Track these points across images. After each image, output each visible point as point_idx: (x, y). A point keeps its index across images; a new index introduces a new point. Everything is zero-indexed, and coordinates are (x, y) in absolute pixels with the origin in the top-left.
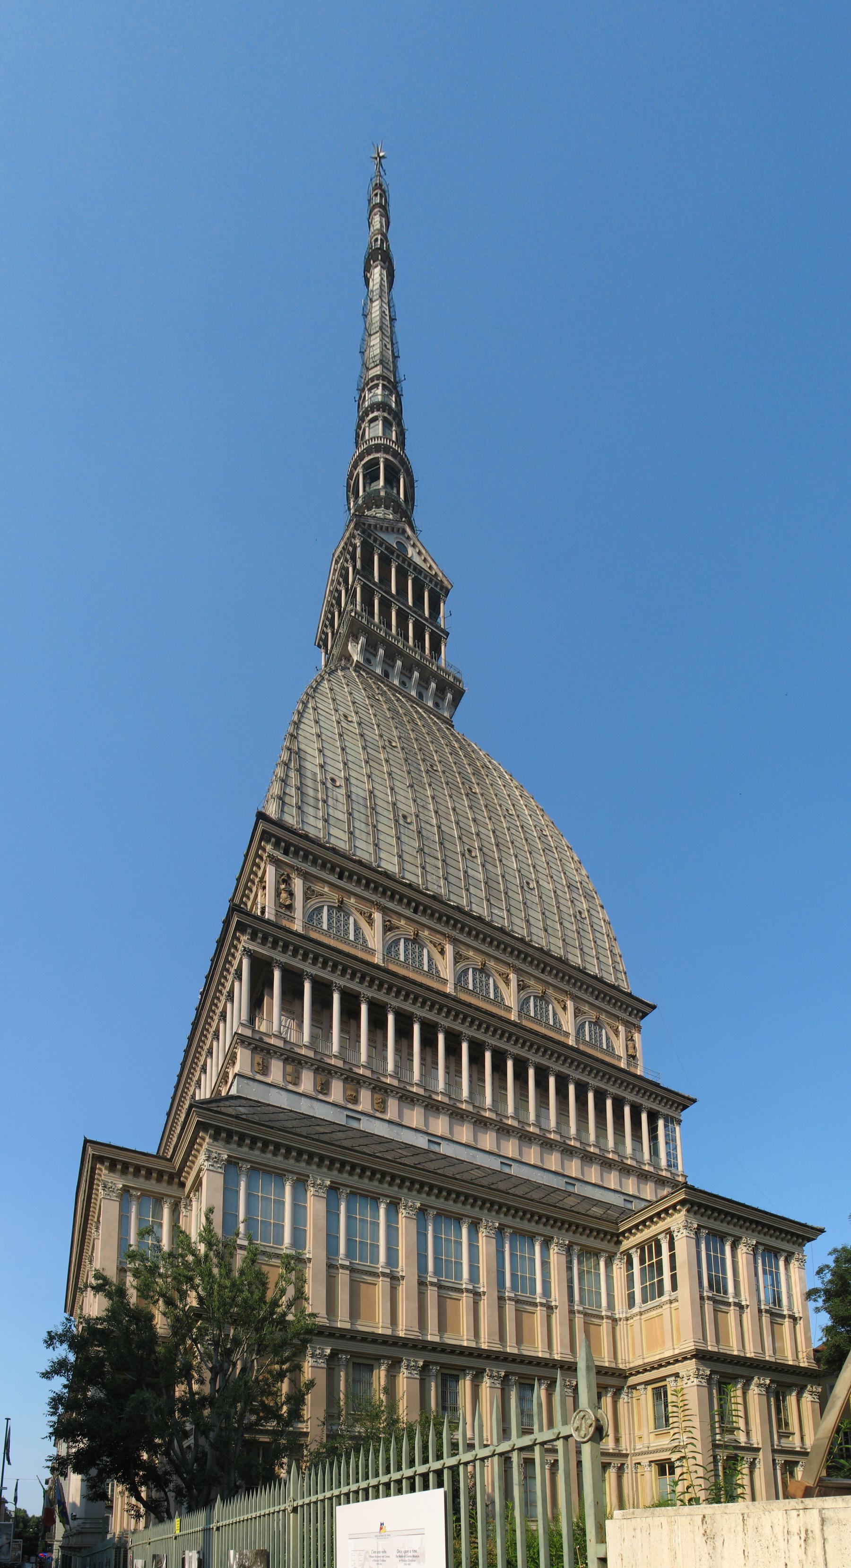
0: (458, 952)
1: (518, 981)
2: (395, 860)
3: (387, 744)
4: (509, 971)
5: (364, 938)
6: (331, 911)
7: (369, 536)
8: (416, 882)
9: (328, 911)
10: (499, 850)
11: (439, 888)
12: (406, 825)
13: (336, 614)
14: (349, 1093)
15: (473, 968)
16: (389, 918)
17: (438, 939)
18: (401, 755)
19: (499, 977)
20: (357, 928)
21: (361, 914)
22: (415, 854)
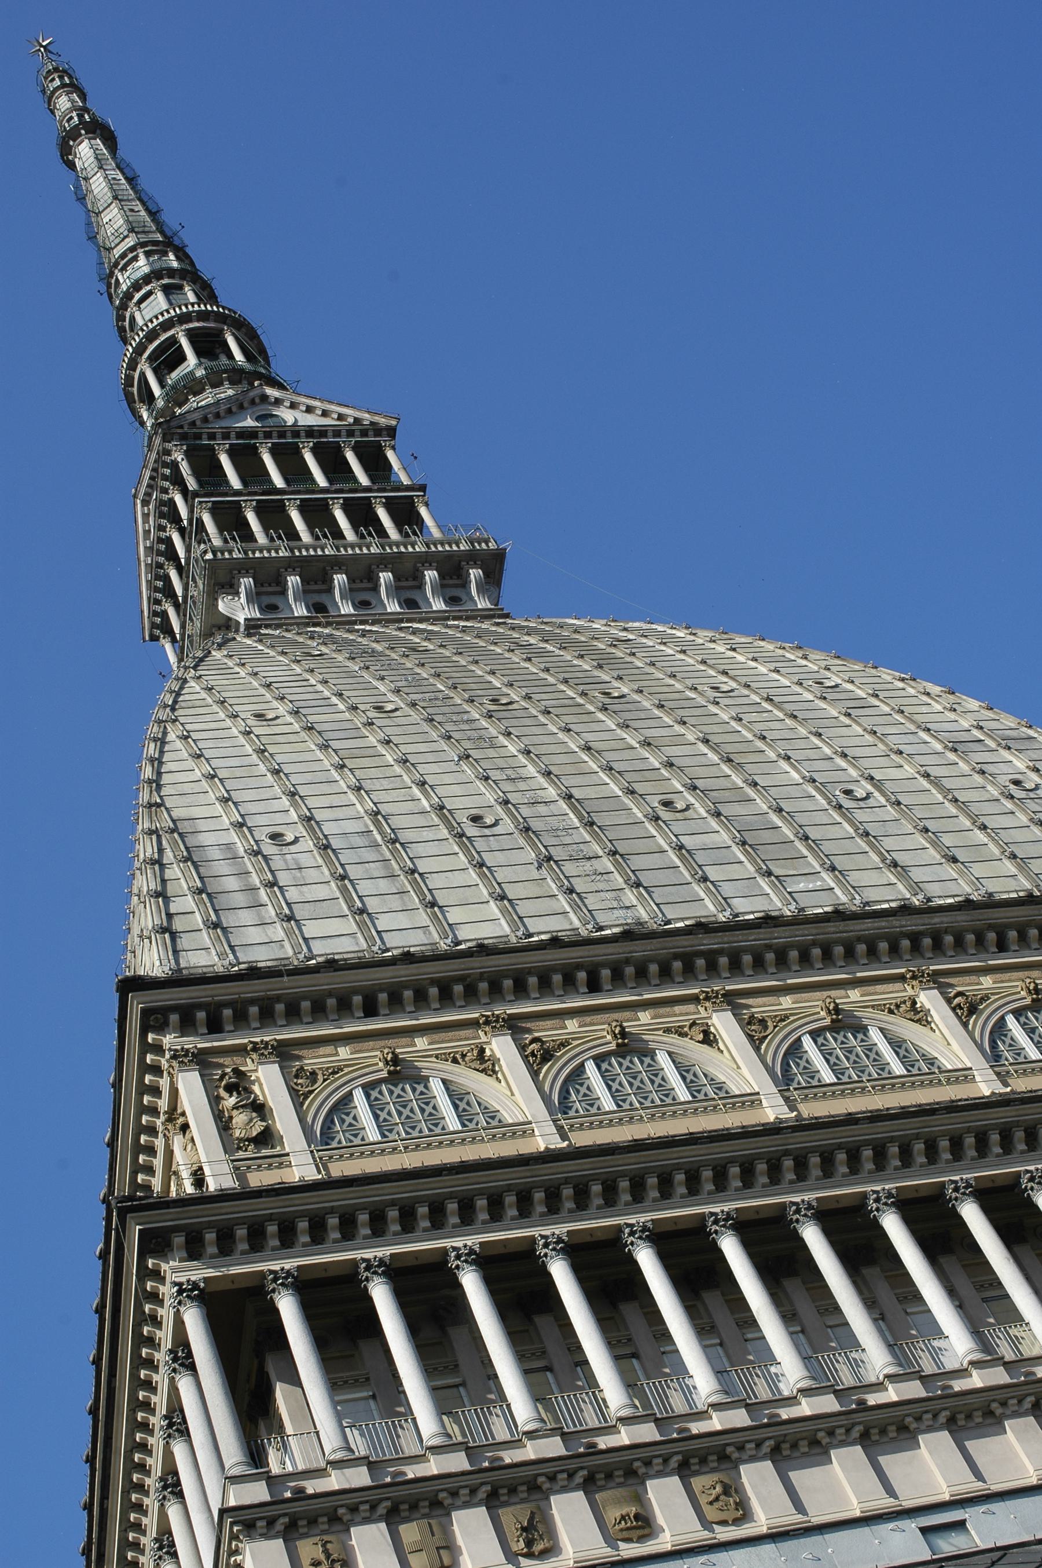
0: (752, 1017)
1: (949, 1001)
2: (493, 909)
3: (372, 714)
4: (910, 992)
5: (485, 1110)
6: (374, 1094)
7: (198, 437)
8: (569, 927)
9: (368, 1096)
10: (738, 767)
11: (629, 913)
12: (487, 832)
13: (173, 574)
14: (613, 1514)
15: (810, 1033)
16: (528, 1037)
17: (682, 1014)
18: (415, 717)
19: (891, 1018)
20: (457, 1096)
21: (455, 1061)
22: (535, 874)
